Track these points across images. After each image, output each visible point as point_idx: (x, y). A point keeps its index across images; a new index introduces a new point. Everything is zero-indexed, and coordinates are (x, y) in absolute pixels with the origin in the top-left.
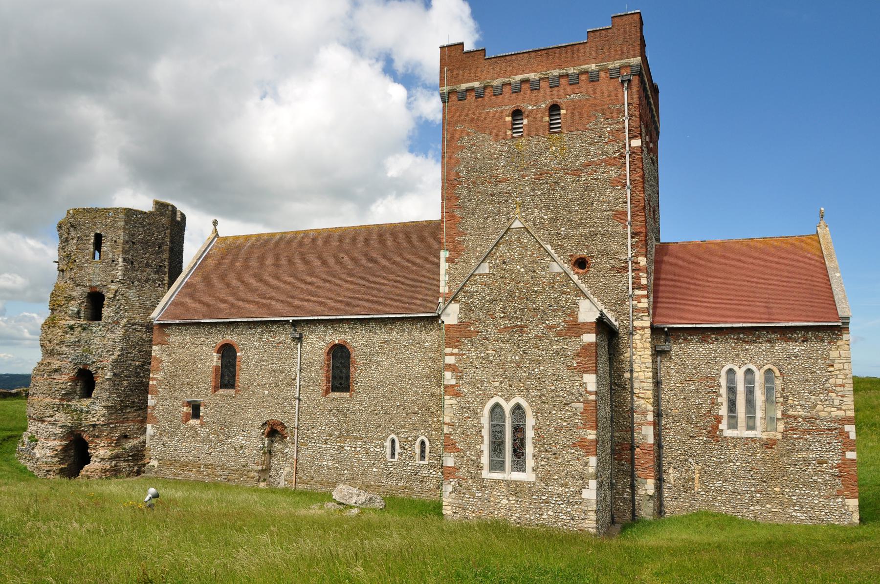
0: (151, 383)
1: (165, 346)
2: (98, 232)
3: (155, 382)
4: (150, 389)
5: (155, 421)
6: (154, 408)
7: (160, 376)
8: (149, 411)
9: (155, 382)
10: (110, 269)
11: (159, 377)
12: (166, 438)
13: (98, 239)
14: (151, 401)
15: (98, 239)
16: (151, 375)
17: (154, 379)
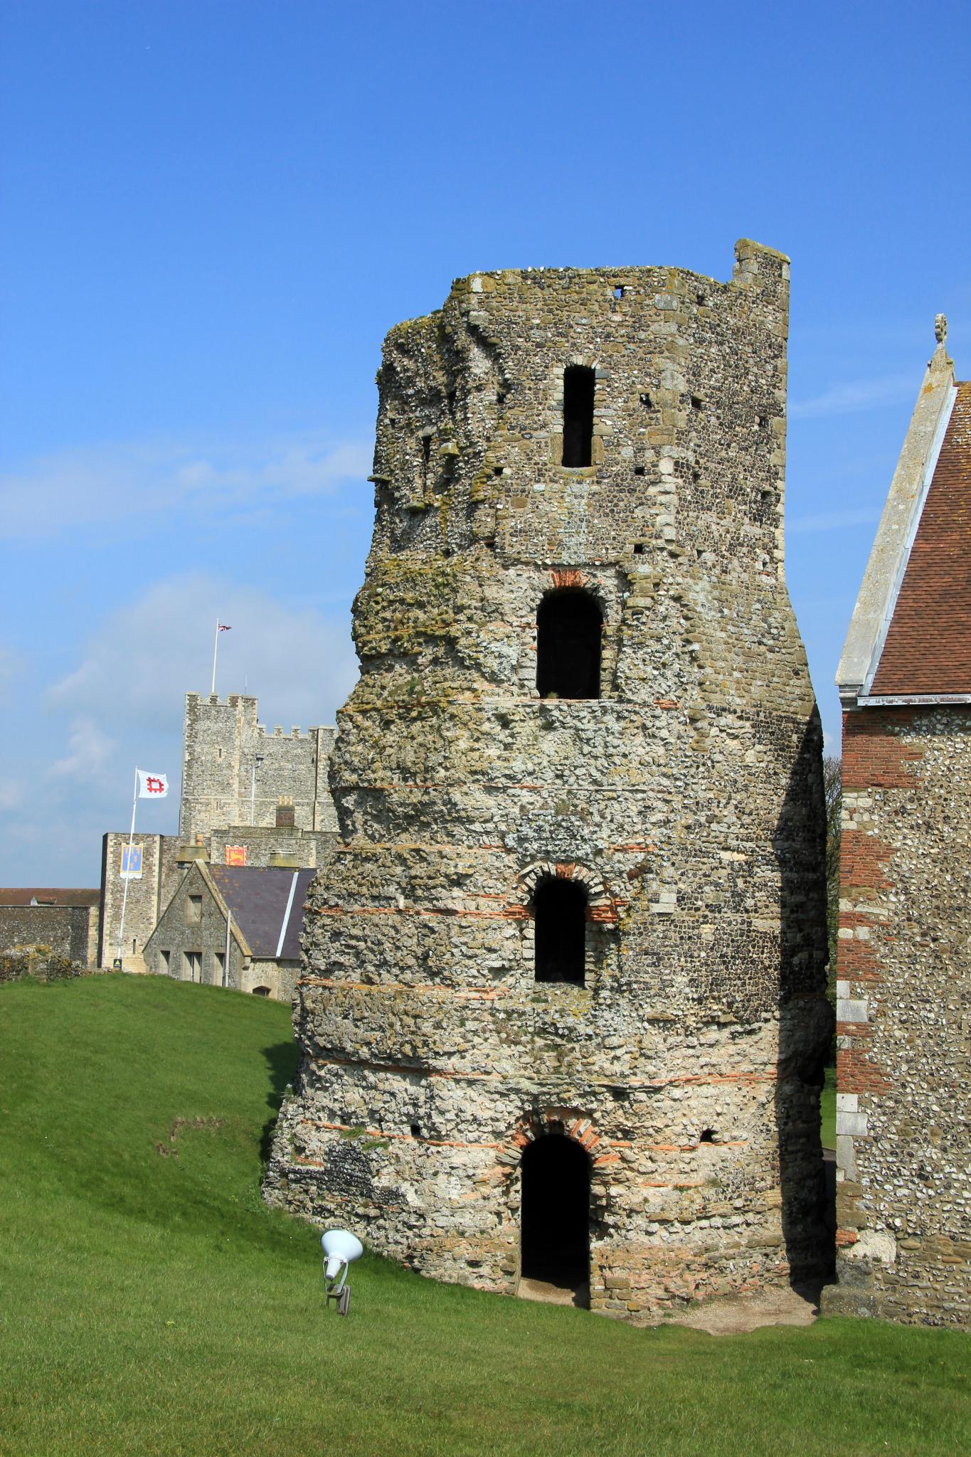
0: (844, 933)
1: (900, 796)
2: (579, 360)
3: (863, 933)
4: (841, 958)
5: (872, 1081)
6: (865, 1031)
7: (885, 908)
8: (844, 1042)
9: (863, 933)
10: (626, 499)
11: (883, 913)
12: (935, 1154)
13: (580, 384)
14: (851, 1005)
15: (580, 384)
16: (845, 905)
17: (856, 920)
